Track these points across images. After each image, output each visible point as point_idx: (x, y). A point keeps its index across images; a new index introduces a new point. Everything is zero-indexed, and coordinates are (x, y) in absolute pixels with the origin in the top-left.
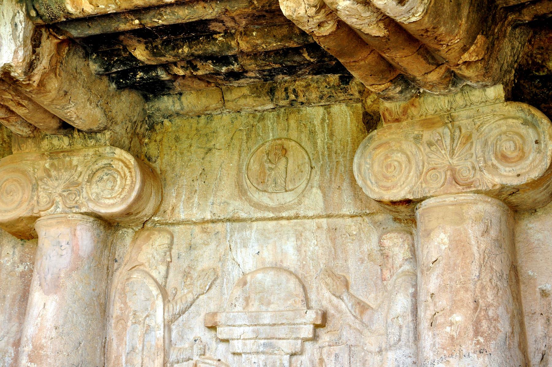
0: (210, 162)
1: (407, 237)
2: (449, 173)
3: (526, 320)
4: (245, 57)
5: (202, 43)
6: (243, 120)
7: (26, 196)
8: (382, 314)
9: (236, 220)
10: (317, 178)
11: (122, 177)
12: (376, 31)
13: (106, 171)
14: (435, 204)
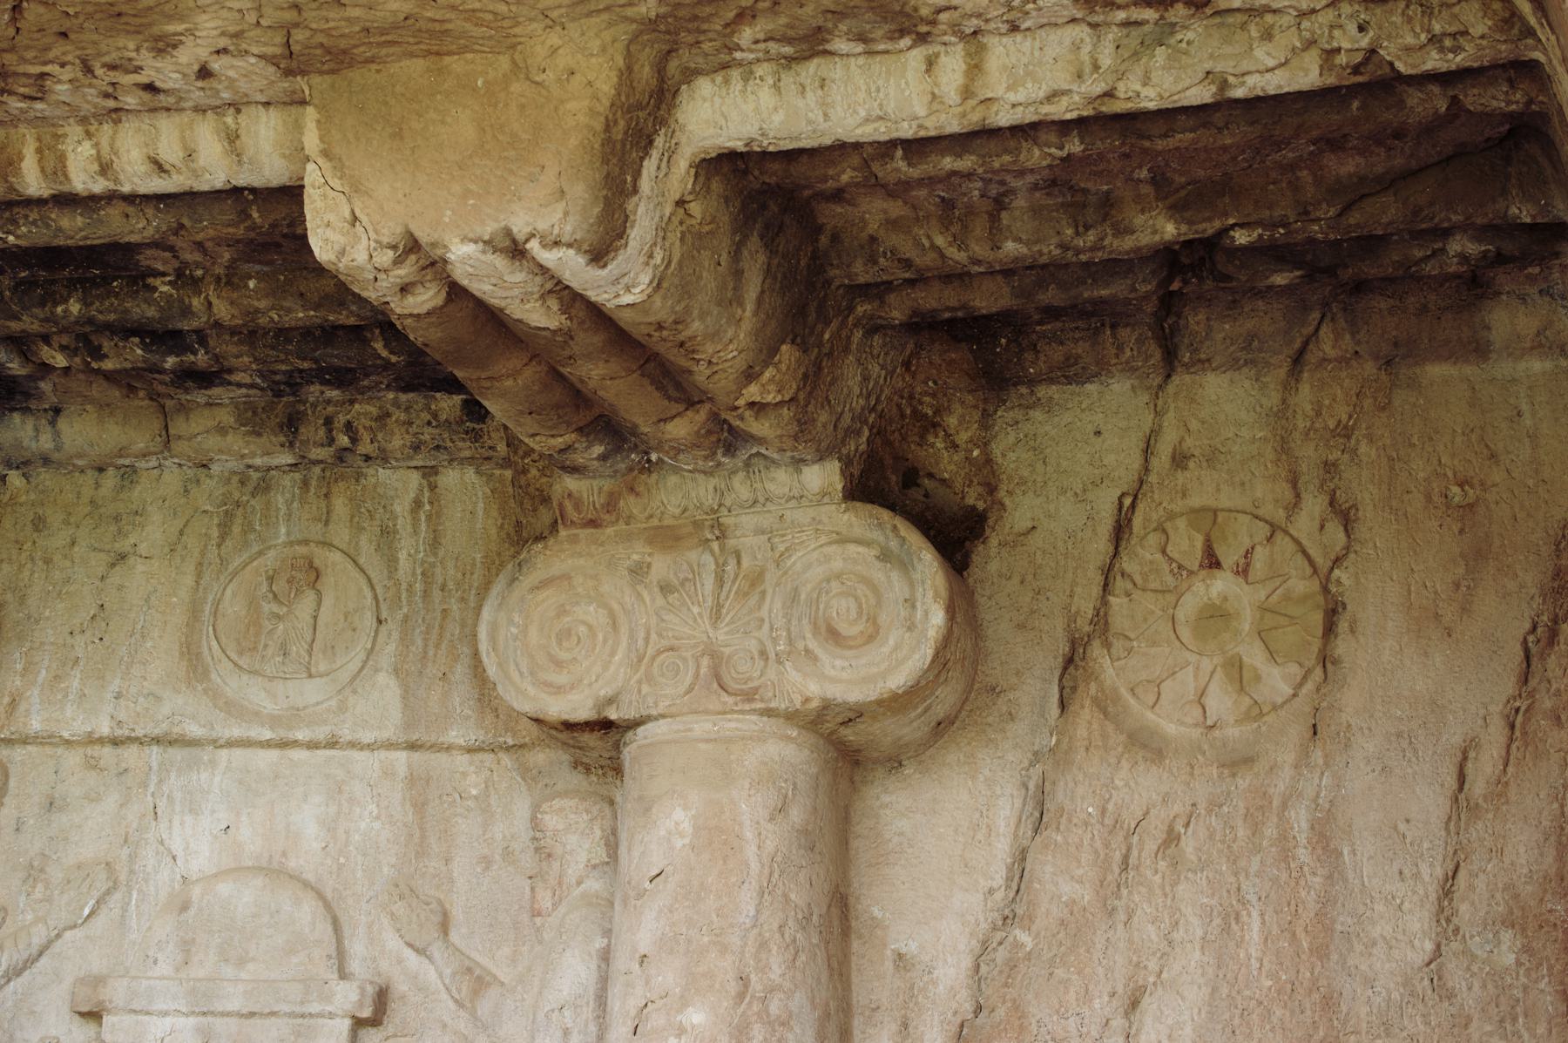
0: (120, 588)
1: (601, 811)
2: (705, 661)
3: (857, 1022)
5: (117, 295)
6: (210, 489)
8: (523, 1000)
9: (176, 741)
10: (391, 648)
12: (539, 316)
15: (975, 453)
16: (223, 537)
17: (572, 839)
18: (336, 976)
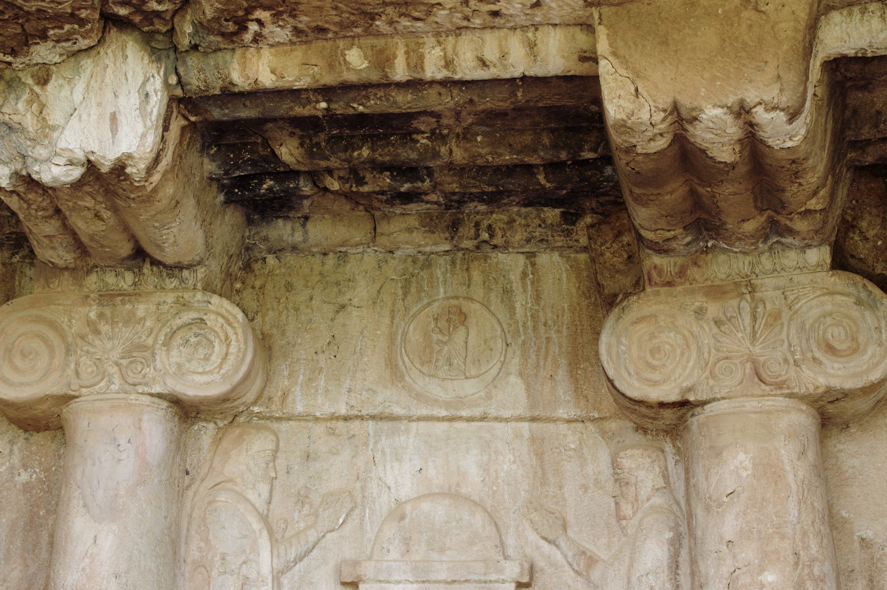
0: (344, 325)
1: (658, 456)
2: (748, 365)
3: (842, 578)
4: (446, 172)
5: (393, 145)
7: (56, 361)
8: (620, 570)
10: (516, 360)
11: (221, 341)
13: (195, 329)
14: (728, 411)
15: (879, 243)
16: (405, 295)
17: (642, 474)
18: (501, 558)
